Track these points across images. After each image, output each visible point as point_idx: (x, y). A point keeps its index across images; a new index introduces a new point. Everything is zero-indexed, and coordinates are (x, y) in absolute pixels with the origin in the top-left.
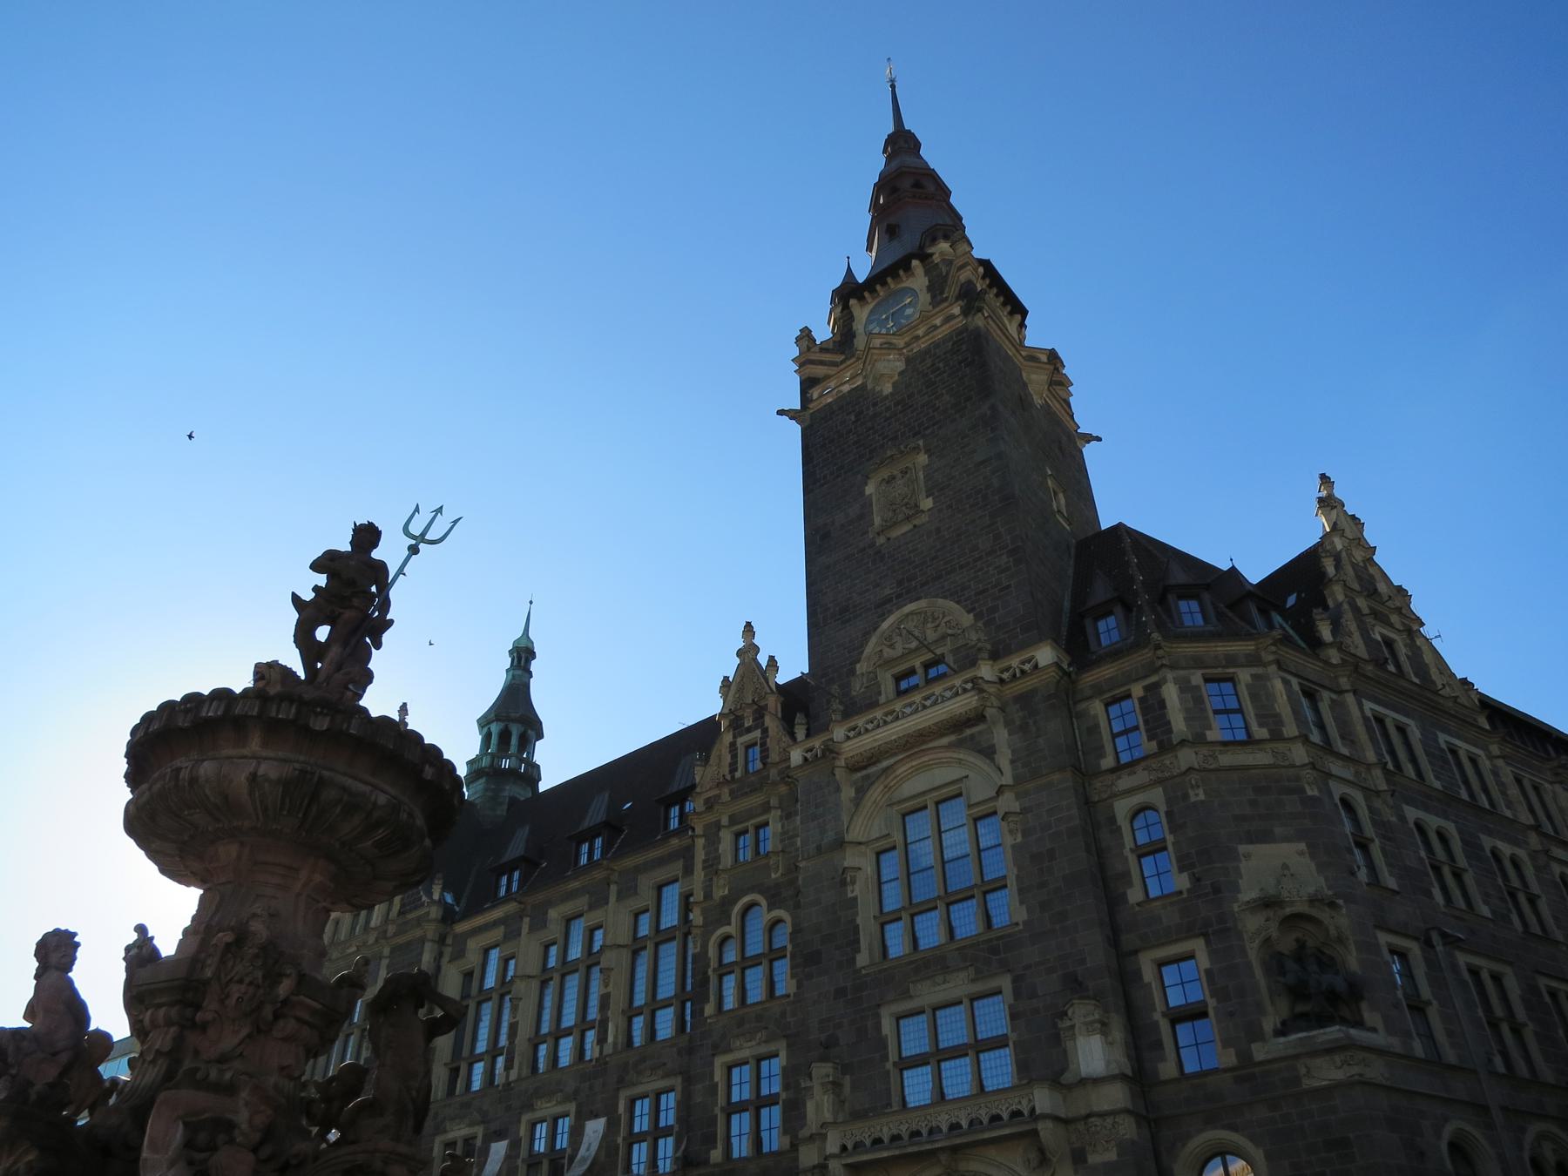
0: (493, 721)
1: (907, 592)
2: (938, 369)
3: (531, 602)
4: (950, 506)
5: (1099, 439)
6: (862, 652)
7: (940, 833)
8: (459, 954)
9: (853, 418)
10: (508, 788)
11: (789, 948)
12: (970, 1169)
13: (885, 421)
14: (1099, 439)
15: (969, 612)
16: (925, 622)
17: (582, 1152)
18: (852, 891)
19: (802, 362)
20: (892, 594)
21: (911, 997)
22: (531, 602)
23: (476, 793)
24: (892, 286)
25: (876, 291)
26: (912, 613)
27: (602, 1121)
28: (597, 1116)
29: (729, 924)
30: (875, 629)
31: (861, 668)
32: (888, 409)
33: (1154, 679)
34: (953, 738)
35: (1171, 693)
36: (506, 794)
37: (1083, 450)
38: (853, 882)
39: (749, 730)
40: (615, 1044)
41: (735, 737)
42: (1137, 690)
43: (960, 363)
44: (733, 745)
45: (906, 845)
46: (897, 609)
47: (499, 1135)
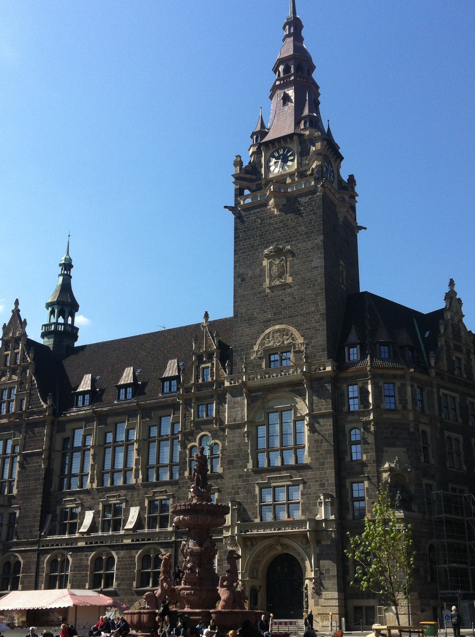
0: (55, 304)
3: (69, 236)
4: (299, 285)
5: (365, 228)
6: (257, 341)
8: (63, 430)
9: (259, 221)
11: (220, 455)
13: (274, 229)
14: (365, 228)
15: (302, 336)
17: (130, 519)
19: (238, 178)
24: (283, 144)
26: (279, 331)
27: (138, 508)
28: (136, 506)
29: (196, 442)
30: (263, 332)
31: (256, 348)
32: (276, 223)
34: (291, 389)
37: (358, 235)
39: (205, 363)
43: (311, 211)
46: (273, 325)
47: (90, 509)
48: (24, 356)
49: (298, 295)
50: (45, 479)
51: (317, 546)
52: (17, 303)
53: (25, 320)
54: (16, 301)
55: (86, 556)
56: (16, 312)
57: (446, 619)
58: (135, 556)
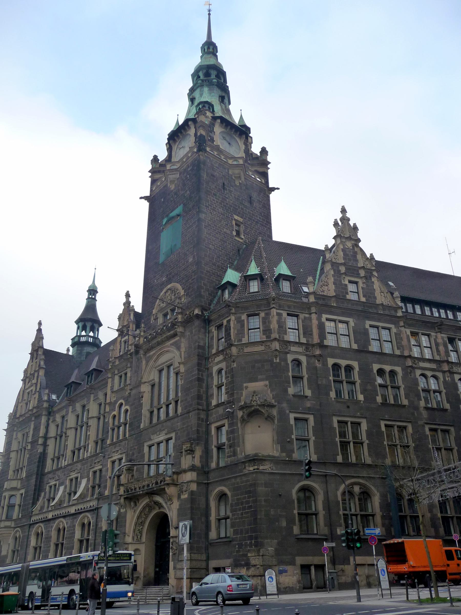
1: (169, 281)
3: (95, 269)
5: (278, 189)
10: (85, 349)
12: (156, 499)
14: (278, 189)
21: (152, 440)
22: (95, 269)
24: (184, 133)
31: (154, 311)
36: (85, 351)
38: (142, 397)
40: (91, 452)
41: (121, 339)
44: (121, 341)
49: (182, 252)
50: (39, 462)
51: (178, 501)
52: (40, 324)
55: (52, 527)
56: (39, 331)
57: (269, 581)
58: (75, 525)
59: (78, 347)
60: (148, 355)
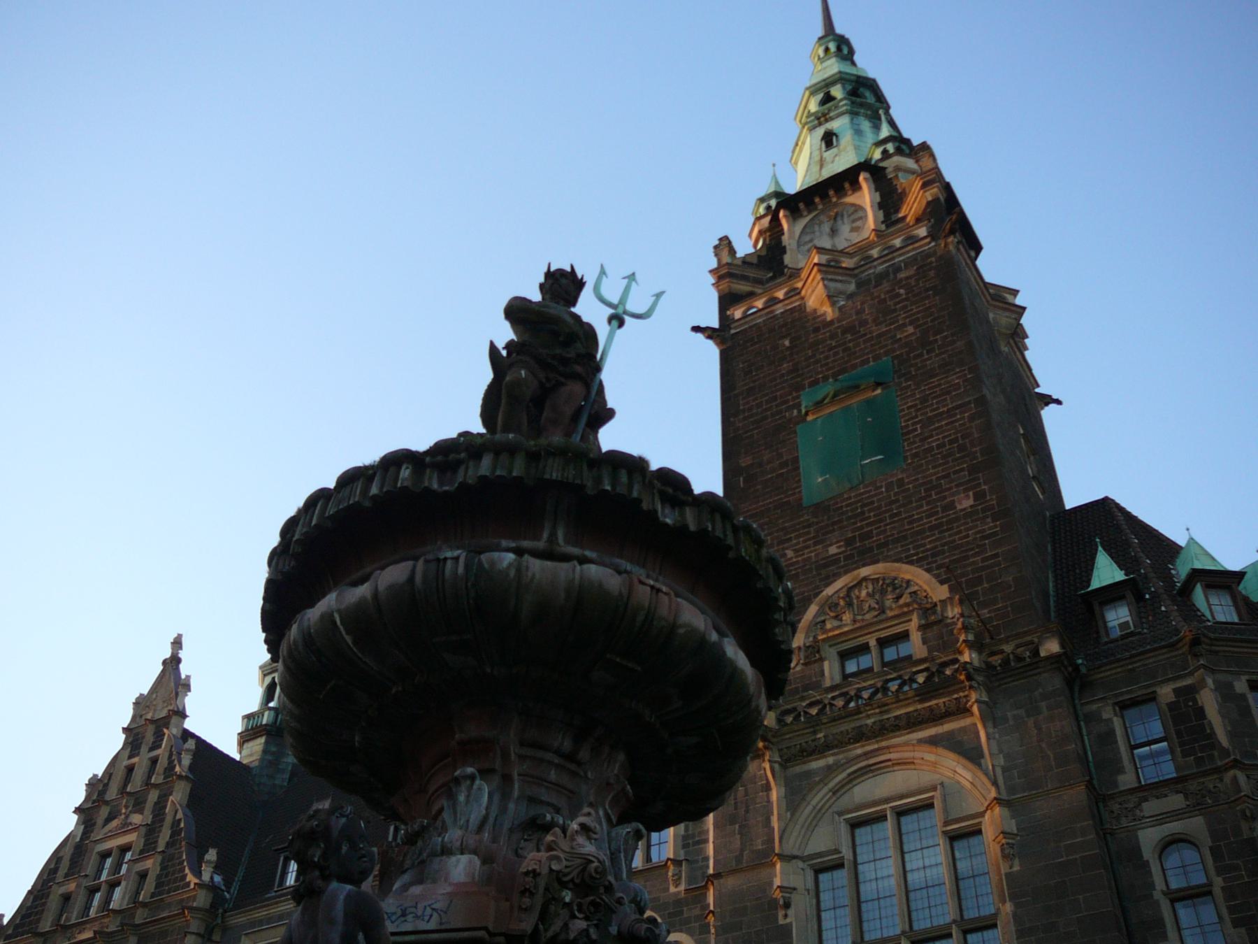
2: (898, 295)
5: (1058, 402)
7: (903, 853)
14: (1058, 402)
15: (942, 583)
16: (883, 592)
18: (786, 916)
20: (840, 553)
23: (251, 755)
24: (834, 200)
25: (814, 203)
26: (865, 579)
30: (817, 595)
33: (1188, 681)
35: (1209, 700)
37: (1043, 412)
42: (1166, 692)
45: (855, 864)
46: (846, 572)
48: (169, 764)
52: (177, 643)
53: (188, 677)
54: (175, 639)
56: (172, 663)
59: (266, 743)
60: (798, 769)
